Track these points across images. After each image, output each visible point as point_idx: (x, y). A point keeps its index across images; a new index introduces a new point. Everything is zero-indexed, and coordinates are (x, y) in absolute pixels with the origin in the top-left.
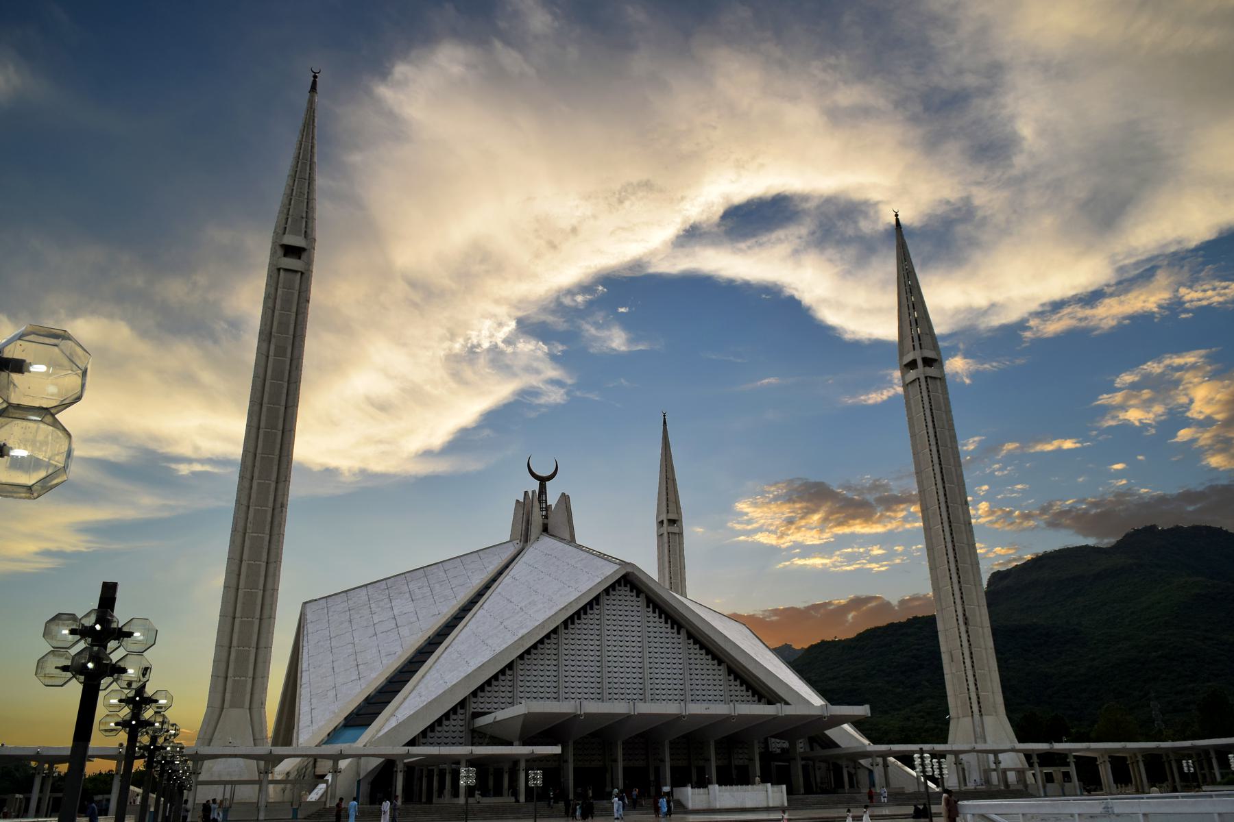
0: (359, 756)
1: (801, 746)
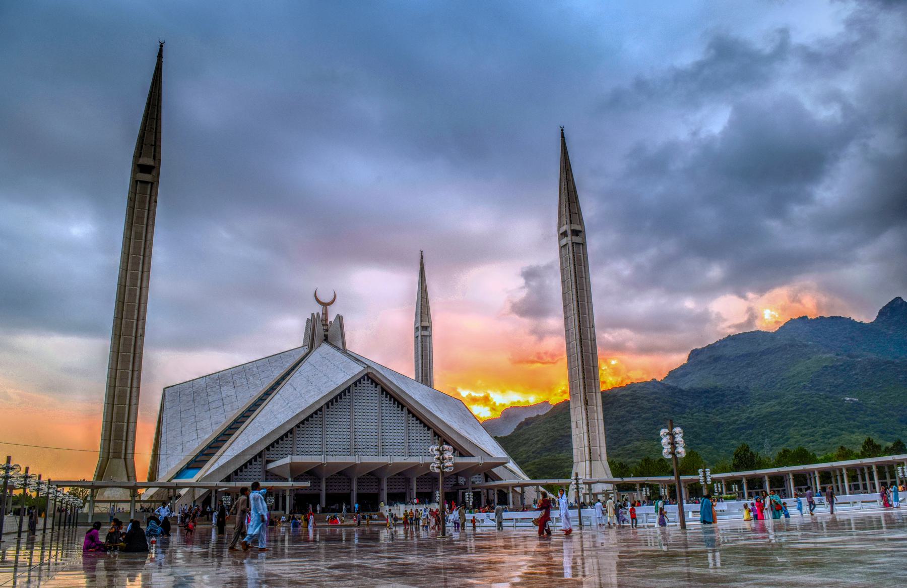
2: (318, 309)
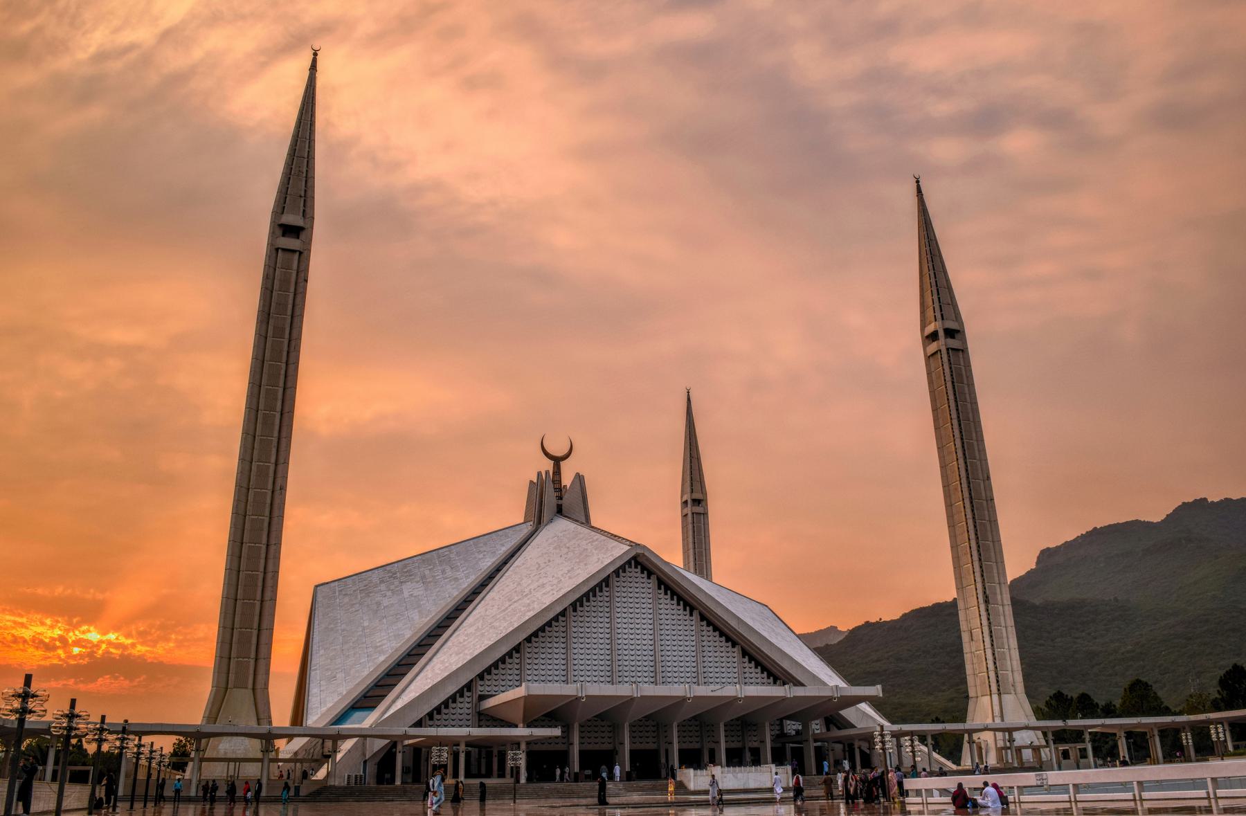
0: (364, 737)
1: (817, 727)
2: (548, 465)
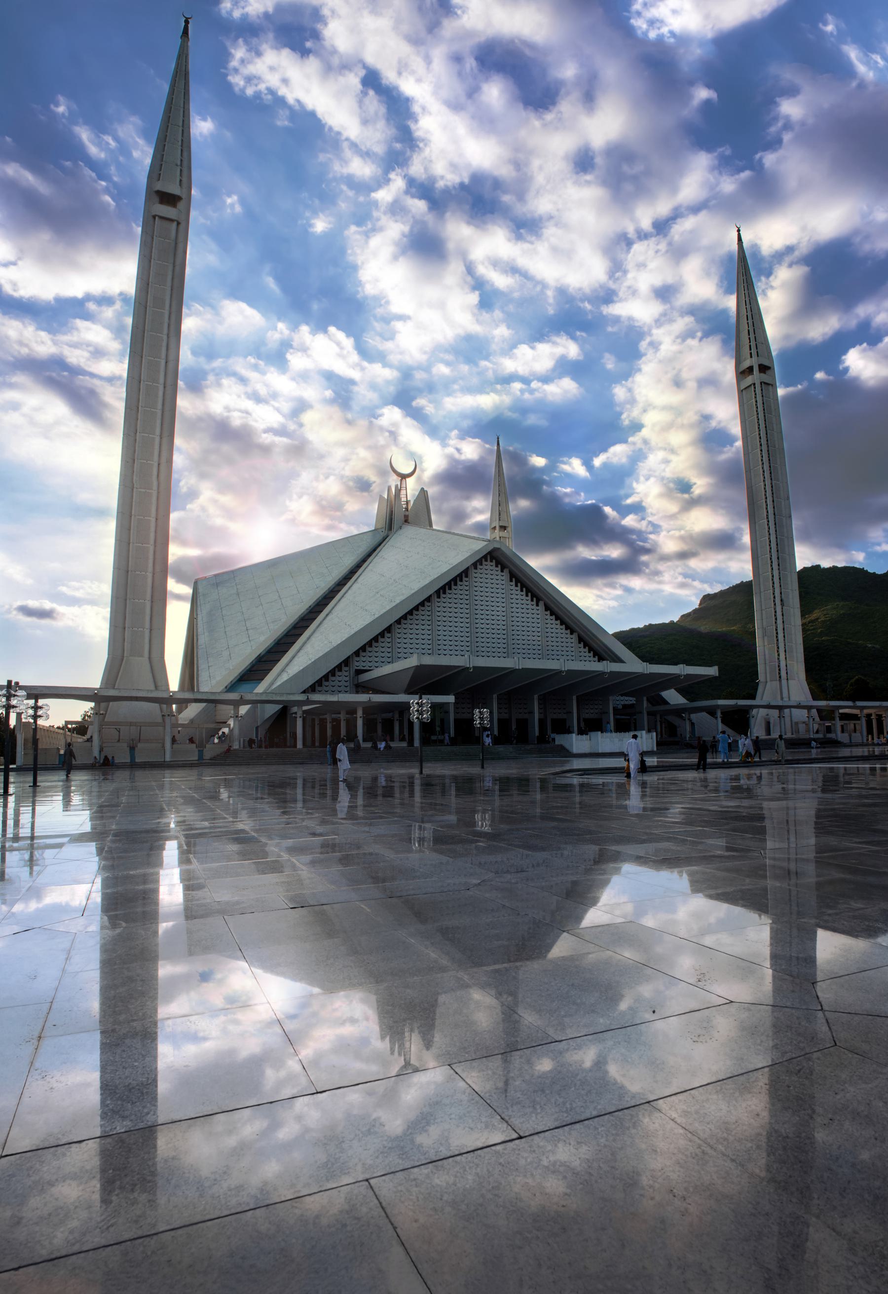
2: (394, 481)
